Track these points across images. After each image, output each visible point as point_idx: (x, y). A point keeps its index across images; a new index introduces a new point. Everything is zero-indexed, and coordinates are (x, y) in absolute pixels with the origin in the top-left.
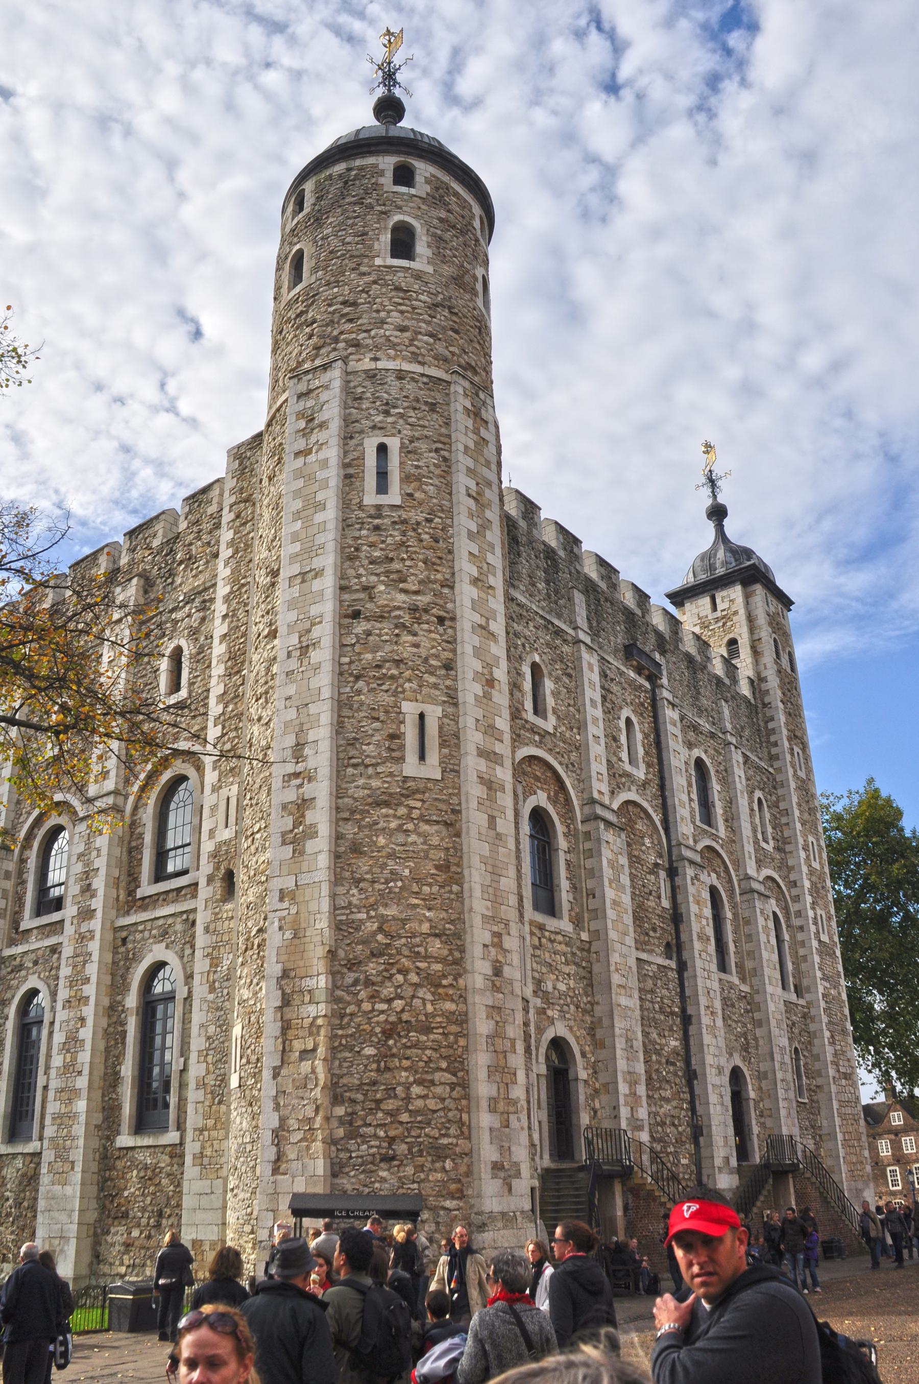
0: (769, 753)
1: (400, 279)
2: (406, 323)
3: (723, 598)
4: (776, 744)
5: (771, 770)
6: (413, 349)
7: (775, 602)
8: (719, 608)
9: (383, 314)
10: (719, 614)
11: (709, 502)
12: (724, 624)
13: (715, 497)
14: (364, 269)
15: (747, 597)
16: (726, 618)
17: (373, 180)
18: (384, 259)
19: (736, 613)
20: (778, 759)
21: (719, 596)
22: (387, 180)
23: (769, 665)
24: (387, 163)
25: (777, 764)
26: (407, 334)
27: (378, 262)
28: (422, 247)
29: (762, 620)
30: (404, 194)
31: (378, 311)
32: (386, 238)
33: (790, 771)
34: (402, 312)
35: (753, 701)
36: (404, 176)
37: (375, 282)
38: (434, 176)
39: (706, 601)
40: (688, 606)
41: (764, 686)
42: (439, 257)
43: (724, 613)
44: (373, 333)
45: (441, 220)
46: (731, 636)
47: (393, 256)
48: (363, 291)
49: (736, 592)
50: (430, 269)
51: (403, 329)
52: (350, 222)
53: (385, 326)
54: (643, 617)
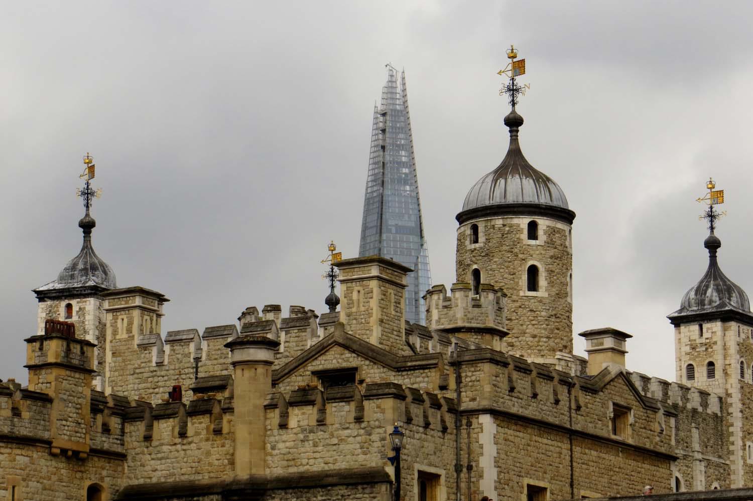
0: (728, 449)
1: (533, 304)
2: (535, 332)
3: (708, 329)
4: (733, 444)
5: (728, 462)
6: (539, 348)
7: (745, 327)
8: (705, 335)
9: (525, 327)
10: (703, 340)
11: (707, 234)
12: (707, 349)
13: (712, 228)
14: (514, 297)
15: (725, 330)
16: (708, 345)
17: (518, 236)
18: (525, 292)
19: (715, 343)
20: (733, 454)
21: (705, 326)
22: (524, 235)
23: (734, 385)
24: (523, 222)
25: (732, 458)
26: (536, 339)
27: (522, 294)
28: (542, 281)
29: (733, 349)
30: (533, 246)
31: (522, 325)
32: (525, 277)
33: (741, 462)
34: (533, 325)
35: (719, 414)
36: (533, 229)
37: (520, 307)
38: (548, 227)
39: (695, 328)
40: (682, 328)
41: (729, 400)
42: (551, 283)
43: (708, 341)
44: (520, 339)
45: (551, 257)
46: (711, 360)
47: (529, 290)
48: (514, 311)
49: (717, 326)
50: (546, 295)
51: (534, 336)
52: (506, 264)
53: (526, 335)
54: (646, 394)
